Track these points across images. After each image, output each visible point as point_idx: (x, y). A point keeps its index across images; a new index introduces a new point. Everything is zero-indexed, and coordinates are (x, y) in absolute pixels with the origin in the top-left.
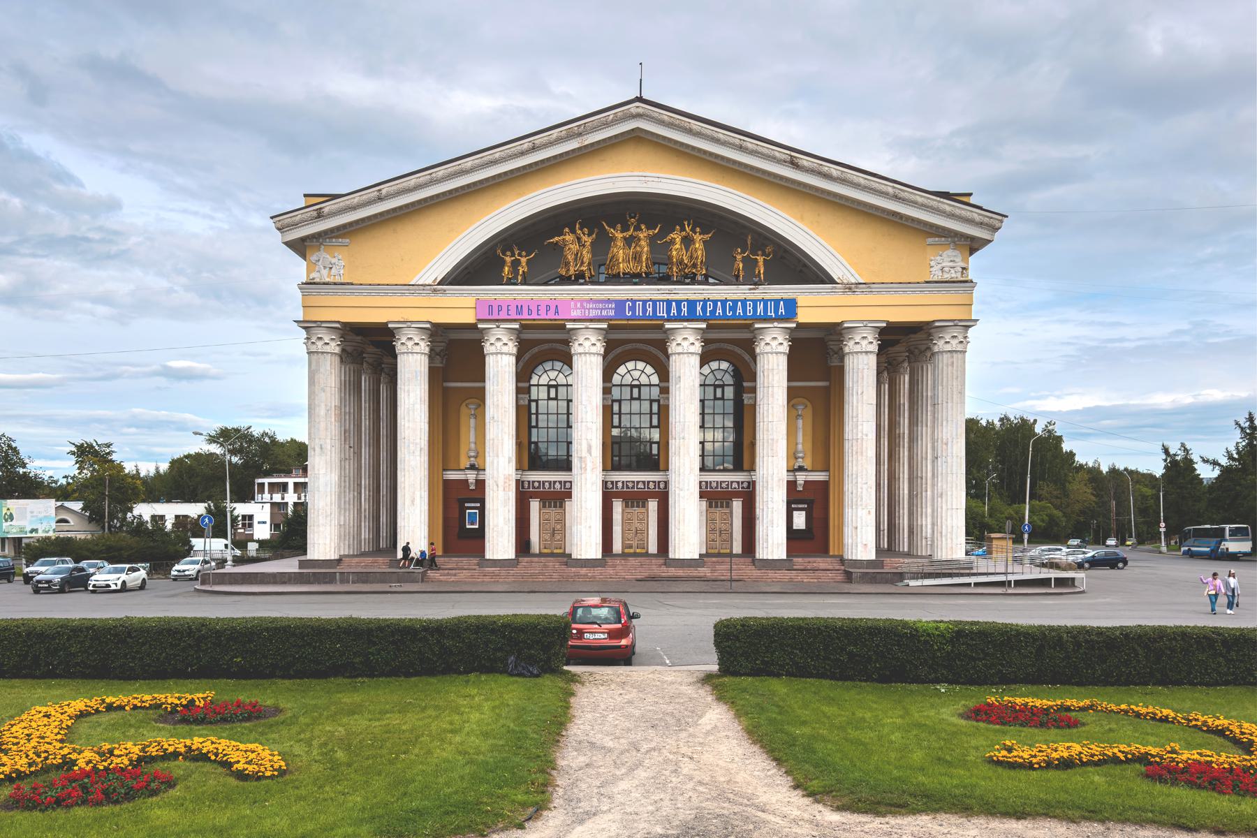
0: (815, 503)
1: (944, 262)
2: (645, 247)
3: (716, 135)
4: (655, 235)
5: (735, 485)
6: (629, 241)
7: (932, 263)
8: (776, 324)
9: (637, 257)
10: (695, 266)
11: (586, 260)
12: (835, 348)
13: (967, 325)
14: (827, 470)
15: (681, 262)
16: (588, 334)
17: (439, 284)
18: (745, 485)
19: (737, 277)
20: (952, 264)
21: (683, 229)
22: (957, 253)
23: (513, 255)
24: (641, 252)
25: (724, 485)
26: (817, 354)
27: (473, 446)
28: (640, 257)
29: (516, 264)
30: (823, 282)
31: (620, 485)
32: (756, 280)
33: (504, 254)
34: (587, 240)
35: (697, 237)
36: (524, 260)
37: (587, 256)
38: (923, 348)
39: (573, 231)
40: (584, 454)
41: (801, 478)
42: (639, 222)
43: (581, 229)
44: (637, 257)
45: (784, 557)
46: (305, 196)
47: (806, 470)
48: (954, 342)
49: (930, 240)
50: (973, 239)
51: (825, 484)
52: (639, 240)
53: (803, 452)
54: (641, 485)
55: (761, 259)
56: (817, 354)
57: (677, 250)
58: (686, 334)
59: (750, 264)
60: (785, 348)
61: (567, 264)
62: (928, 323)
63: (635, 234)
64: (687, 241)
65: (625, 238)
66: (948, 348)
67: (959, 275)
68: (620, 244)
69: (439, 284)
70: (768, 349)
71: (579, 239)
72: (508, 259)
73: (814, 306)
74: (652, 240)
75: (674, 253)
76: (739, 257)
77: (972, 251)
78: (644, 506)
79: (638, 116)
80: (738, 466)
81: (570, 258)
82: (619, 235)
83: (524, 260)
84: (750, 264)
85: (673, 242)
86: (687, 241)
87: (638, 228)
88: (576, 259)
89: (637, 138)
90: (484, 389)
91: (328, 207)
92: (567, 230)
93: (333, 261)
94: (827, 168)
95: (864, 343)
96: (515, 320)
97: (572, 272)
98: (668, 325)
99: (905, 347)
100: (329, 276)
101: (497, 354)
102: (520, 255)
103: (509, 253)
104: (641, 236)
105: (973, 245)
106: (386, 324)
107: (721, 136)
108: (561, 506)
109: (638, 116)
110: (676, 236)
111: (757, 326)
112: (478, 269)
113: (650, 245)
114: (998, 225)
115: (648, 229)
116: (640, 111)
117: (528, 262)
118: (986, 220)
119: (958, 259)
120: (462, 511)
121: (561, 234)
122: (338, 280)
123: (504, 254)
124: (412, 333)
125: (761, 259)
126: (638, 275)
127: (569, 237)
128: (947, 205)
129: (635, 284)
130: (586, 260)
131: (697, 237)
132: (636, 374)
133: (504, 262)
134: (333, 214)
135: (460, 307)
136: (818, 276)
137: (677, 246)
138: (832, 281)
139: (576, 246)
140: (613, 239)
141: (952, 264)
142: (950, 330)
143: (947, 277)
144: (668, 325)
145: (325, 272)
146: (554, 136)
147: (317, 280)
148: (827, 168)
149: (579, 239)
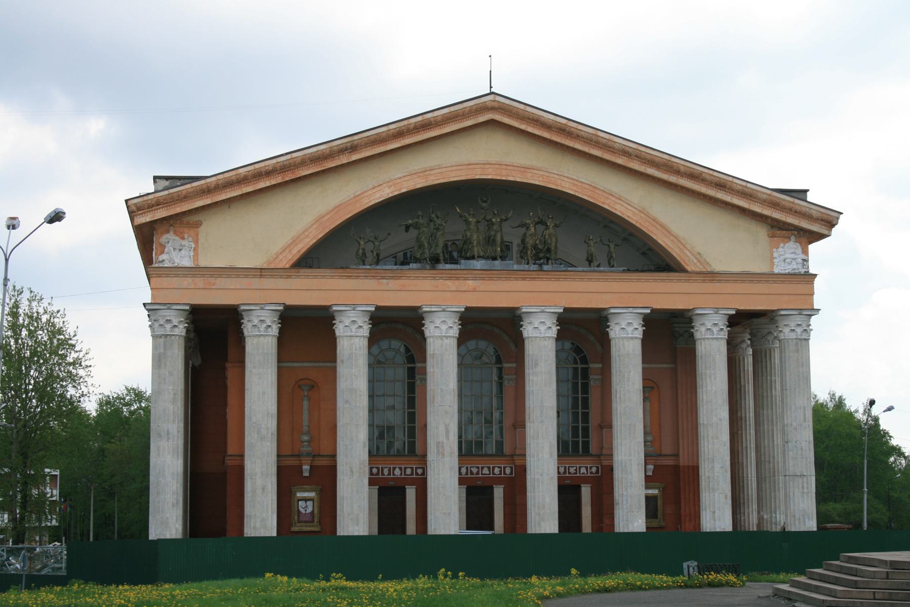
20: (793, 256)
28: (494, 241)
46: (155, 178)
48: (799, 330)
60: (639, 334)
67: (800, 266)
73: (665, 293)
112: (329, 251)
136: (667, 265)
141: (793, 256)
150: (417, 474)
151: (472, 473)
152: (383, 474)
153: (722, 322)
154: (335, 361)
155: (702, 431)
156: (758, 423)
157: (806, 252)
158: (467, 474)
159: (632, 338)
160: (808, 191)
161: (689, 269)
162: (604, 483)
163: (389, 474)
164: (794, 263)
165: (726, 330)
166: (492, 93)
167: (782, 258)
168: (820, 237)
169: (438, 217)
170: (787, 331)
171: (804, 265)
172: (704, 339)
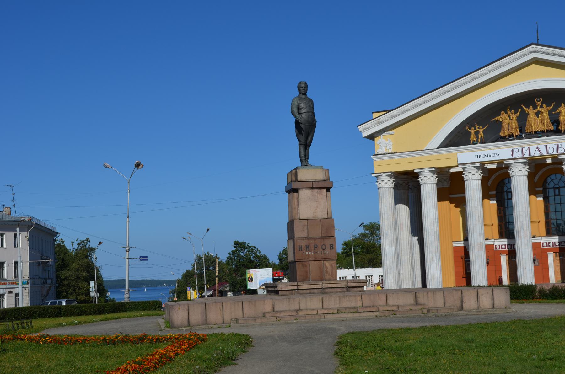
2: (546, 115)
6: (537, 114)
9: (542, 121)
11: (514, 127)
17: (438, 148)
23: (475, 128)
24: (544, 119)
29: (477, 133)
31: (551, 244)
34: (514, 117)
36: (481, 131)
37: (515, 124)
39: (506, 113)
42: (542, 103)
61: (504, 130)
65: (536, 113)
69: (438, 148)
72: (473, 131)
74: (550, 112)
75: (562, 118)
85: (560, 112)
87: (541, 107)
93: (387, 142)
97: (506, 134)
100: (386, 150)
102: (479, 128)
109: (534, 52)
112: (459, 137)
115: (547, 106)
116: (533, 49)
117: (484, 132)
121: (499, 114)
122: (390, 151)
123: (470, 129)
126: (543, 132)
129: (540, 137)
130: (514, 127)
133: (470, 133)
140: (528, 114)
145: (384, 148)
147: (380, 153)
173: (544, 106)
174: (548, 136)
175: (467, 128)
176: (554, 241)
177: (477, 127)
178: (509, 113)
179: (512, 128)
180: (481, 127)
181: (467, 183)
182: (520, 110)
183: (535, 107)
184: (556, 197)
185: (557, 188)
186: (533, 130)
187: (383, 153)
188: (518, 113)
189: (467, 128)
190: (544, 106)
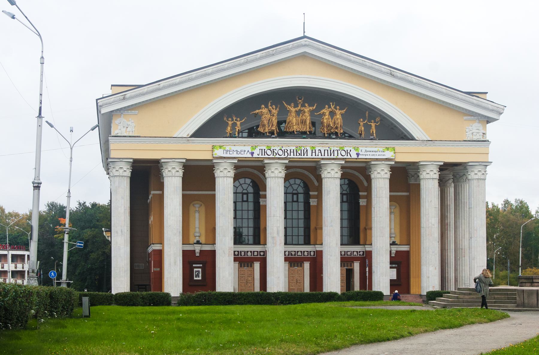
0: (402, 262)
1: (473, 130)
3: (349, 58)
4: (313, 110)
5: (355, 253)
6: (298, 113)
7: (467, 130)
8: (383, 162)
10: (337, 128)
12: (413, 173)
13: (486, 164)
14: (408, 244)
15: (329, 126)
16: (276, 166)
17: (190, 137)
18: (361, 253)
19: (361, 134)
20: (477, 131)
21: (330, 107)
22: (480, 125)
23: (233, 120)
25: (349, 253)
26: (404, 178)
27: (197, 230)
28: (305, 122)
29: (234, 125)
30: (408, 139)
32: (372, 137)
33: (228, 120)
34: (275, 112)
35: (338, 112)
36: (238, 123)
38: (462, 174)
39: (267, 107)
40: (275, 235)
41: (395, 249)
42: (304, 102)
43: (271, 106)
44: (303, 122)
45: (389, 294)
46: (112, 86)
47: (397, 244)
48: (480, 174)
49: (465, 118)
50: (488, 117)
51: (407, 253)
52: (304, 112)
53: (395, 234)
54: (299, 254)
55: (373, 125)
56: (404, 178)
57: (326, 119)
58: (333, 167)
59: (368, 127)
60: (388, 176)
62: (465, 163)
63: (302, 109)
64: (332, 114)
65: (296, 111)
66: (476, 177)
67: (481, 137)
68: (293, 114)
69: (190, 137)
70: (379, 176)
71: (270, 111)
72: (230, 123)
73: (403, 152)
74: (312, 113)
75: (325, 121)
76: (361, 124)
77: (488, 122)
78: (301, 266)
79: (305, 45)
80: (307, 242)
81: (266, 122)
82: (293, 110)
83: (238, 123)
84: (368, 127)
85: (324, 114)
86: (332, 114)
87: (303, 105)
88: (268, 123)
89: (304, 56)
90: (214, 195)
91: (129, 94)
92: (263, 106)
93: (129, 123)
94: (410, 77)
95: (432, 173)
96: (234, 158)
97: (267, 130)
98: (323, 162)
99: (452, 174)
100: (126, 131)
101: (224, 177)
102: (236, 120)
103: (230, 119)
104: (306, 110)
105: (489, 120)
106: (160, 160)
107: (352, 58)
108: (251, 266)
109: (305, 45)
110: (326, 111)
111: (373, 163)
113: (311, 115)
114: (501, 112)
115: (309, 106)
116: (307, 43)
118: (495, 109)
119: (481, 128)
120: (192, 269)
124: (175, 165)
125: (373, 125)
126: (304, 133)
127: (265, 111)
128: (474, 99)
129: (304, 138)
131: (338, 112)
132: (295, 187)
133: (228, 123)
134: (132, 98)
135: (202, 150)
136: (405, 136)
137: (327, 117)
138: (413, 139)
139: (268, 116)
140: (289, 111)
141: (477, 131)
142: (477, 167)
143: (475, 138)
144: (323, 162)
146: (259, 56)
148: (410, 77)
149: (270, 111)
150: (260, 255)
151: (292, 255)
152: (241, 255)
153: (436, 170)
154: (215, 191)
155: (423, 231)
156: (456, 228)
157: (485, 128)
158: (289, 255)
159: (384, 178)
160: (487, 93)
161: (417, 139)
162: (366, 260)
163: (245, 255)
164: (478, 135)
165: (438, 174)
166: (305, 37)
167: (471, 132)
168: (495, 120)
169: (273, 109)
170: (473, 174)
171: (483, 136)
172: (425, 179)
173: (306, 105)
174: (311, 138)
175: (225, 119)
176: (290, 250)
177: (235, 119)
178: (270, 107)
179: (272, 125)
180: (238, 119)
181: (217, 180)
182: (279, 106)
183: (296, 106)
184: (243, 203)
185: (245, 194)
186: (295, 130)
187: (123, 135)
188: (278, 109)
189: (225, 119)
190: (306, 105)
